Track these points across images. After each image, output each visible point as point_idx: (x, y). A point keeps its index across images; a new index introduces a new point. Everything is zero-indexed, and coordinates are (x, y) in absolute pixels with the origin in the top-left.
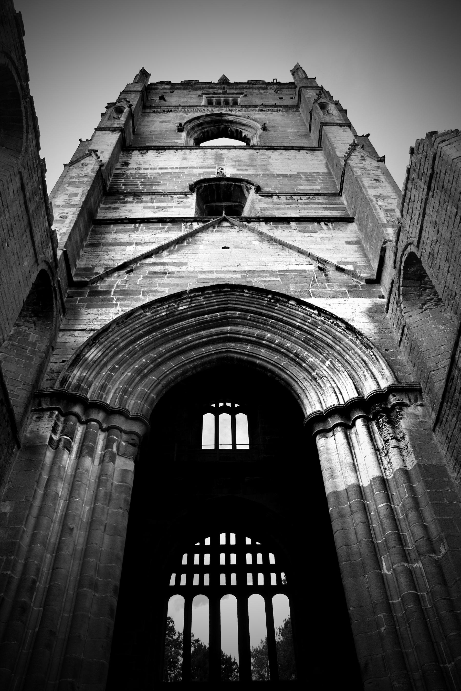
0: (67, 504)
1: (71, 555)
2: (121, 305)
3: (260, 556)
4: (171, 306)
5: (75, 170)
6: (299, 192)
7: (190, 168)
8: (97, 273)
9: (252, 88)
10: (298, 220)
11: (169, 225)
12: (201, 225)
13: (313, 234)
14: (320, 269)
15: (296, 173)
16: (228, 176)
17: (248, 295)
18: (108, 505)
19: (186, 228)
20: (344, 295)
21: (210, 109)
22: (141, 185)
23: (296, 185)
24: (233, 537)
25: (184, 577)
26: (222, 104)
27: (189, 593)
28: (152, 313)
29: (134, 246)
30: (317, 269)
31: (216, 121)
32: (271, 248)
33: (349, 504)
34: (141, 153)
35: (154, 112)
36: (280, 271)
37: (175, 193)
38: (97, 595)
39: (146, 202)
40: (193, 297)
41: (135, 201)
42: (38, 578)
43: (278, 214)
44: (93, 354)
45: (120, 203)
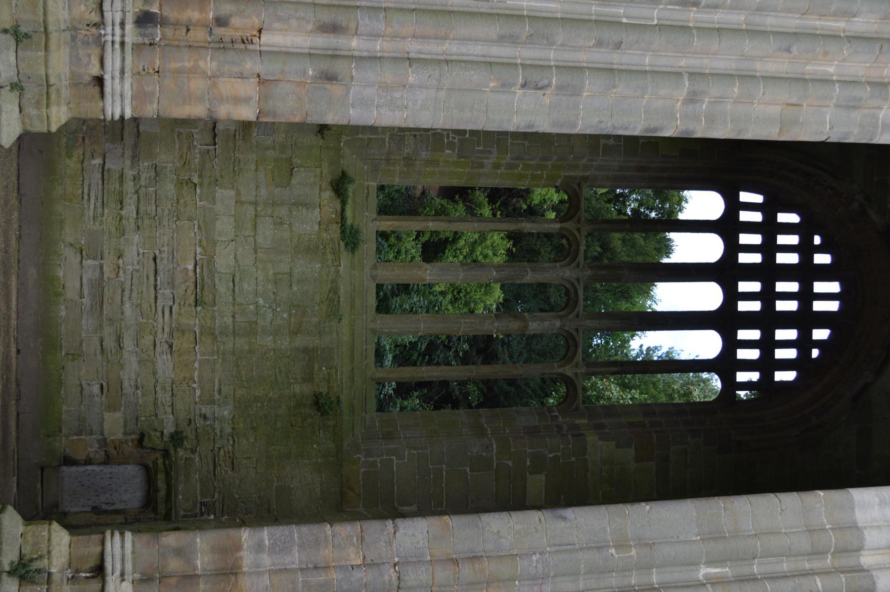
0: (838, 33)
1: (743, 55)
3: (791, 354)
18: (836, 106)
24: (833, 306)
25: (756, 217)
27: (727, 227)
33: (828, 526)
38: (679, 104)
42: (704, 7)
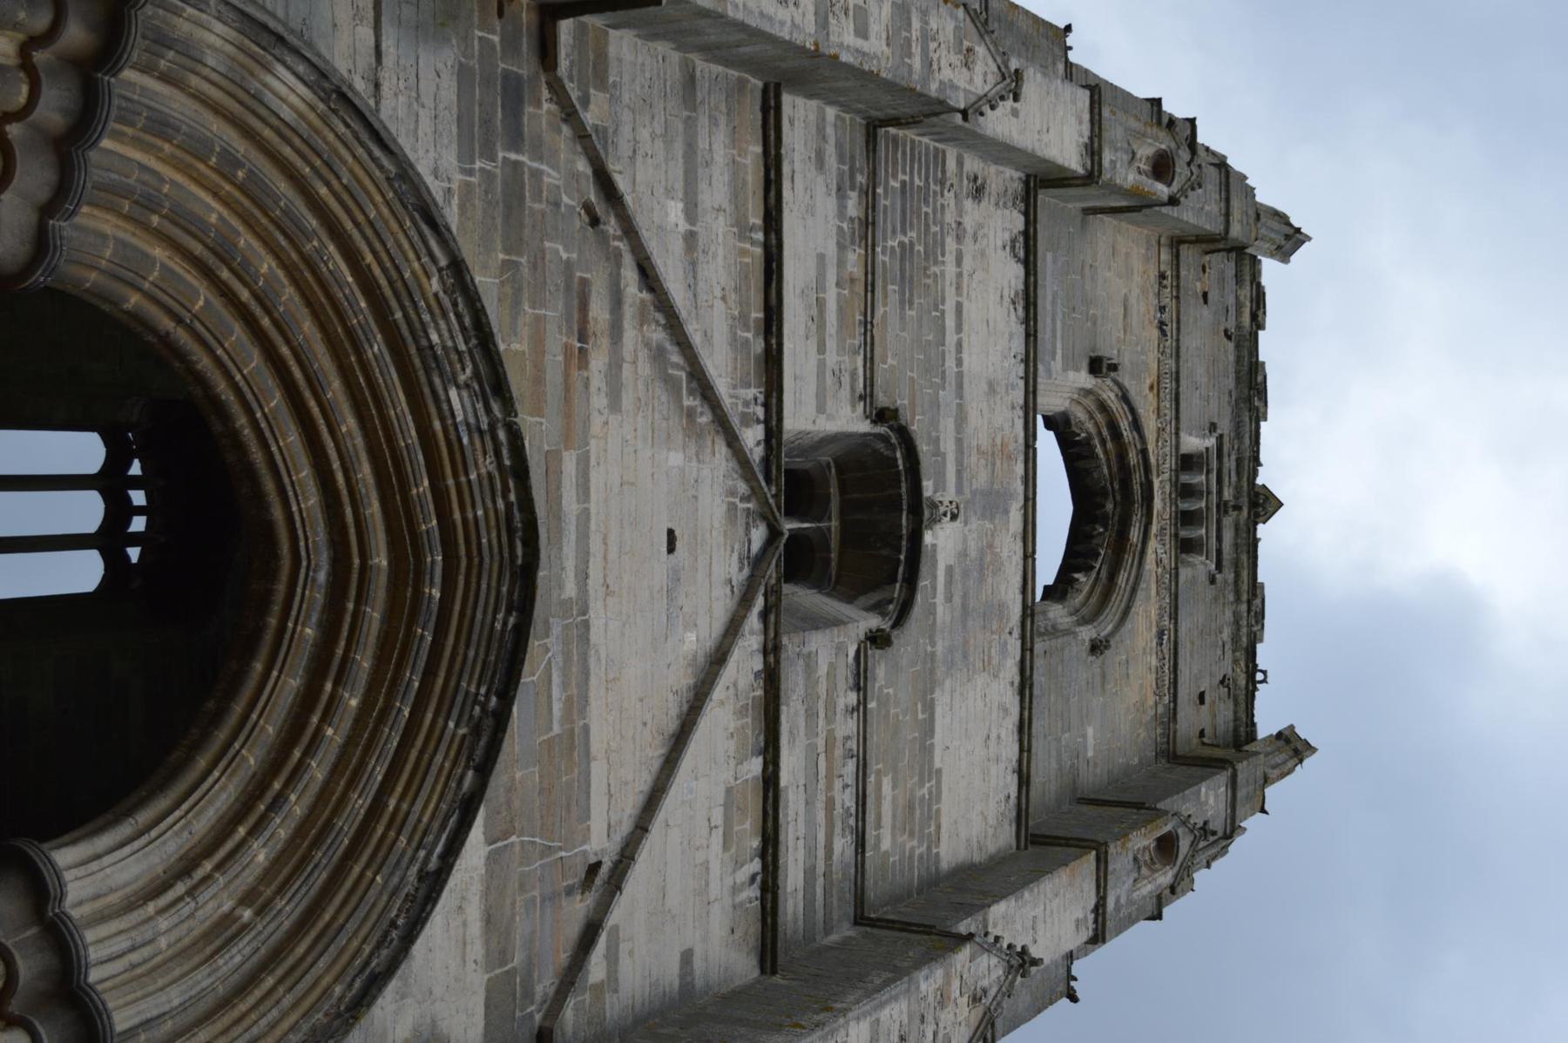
2: (467, 188)
4: (461, 361)
5: (950, 26)
6: (872, 779)
7: (960, 406)
8: (585, 101)
9: (1238, 599)
10: (770, 782)
11: (758, 346)
12: (757, 454)
13: (717, 838)
14: (594, 869)
15: (937, 764)
16: (928, 538)
17: (498, 626)
19: (746, 404)
20: (497, 954)
21: (1169, 464)
22: (901, 244)
23: (895, 771)
26: (1185, 506)
28: (436, 295)
29: (683, 226)
30: (593, 860)
31: (1126, 483)
32: (671, 697)
34: (1013, 241)
35: (1162, 276)
36: (586, 729)
37: (869, 362)
39: (841, 263)
40: (494, 438)
41: (845, 226)
43: (791, 715)
44: (286, 90)
45: (841, 174)
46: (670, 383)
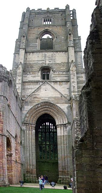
13: (62, 86)
44: (28, 115)
46: (38, 90)
